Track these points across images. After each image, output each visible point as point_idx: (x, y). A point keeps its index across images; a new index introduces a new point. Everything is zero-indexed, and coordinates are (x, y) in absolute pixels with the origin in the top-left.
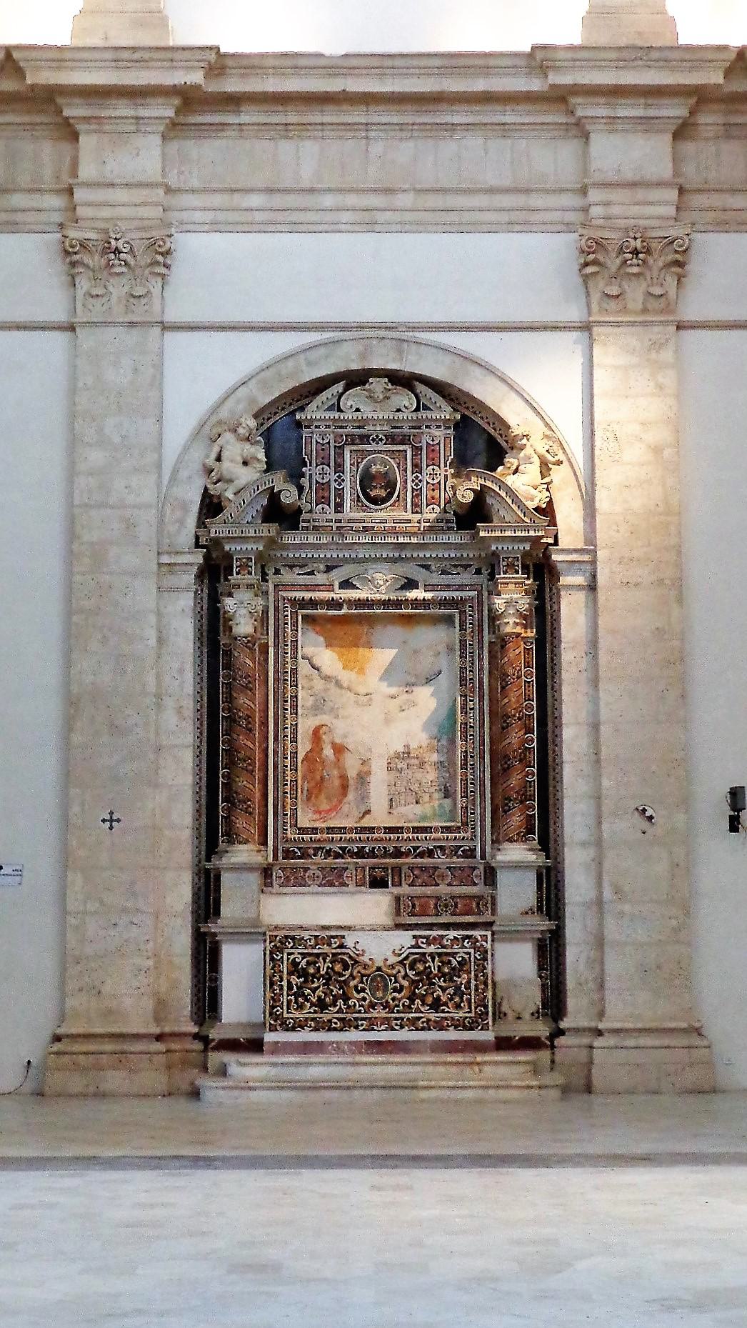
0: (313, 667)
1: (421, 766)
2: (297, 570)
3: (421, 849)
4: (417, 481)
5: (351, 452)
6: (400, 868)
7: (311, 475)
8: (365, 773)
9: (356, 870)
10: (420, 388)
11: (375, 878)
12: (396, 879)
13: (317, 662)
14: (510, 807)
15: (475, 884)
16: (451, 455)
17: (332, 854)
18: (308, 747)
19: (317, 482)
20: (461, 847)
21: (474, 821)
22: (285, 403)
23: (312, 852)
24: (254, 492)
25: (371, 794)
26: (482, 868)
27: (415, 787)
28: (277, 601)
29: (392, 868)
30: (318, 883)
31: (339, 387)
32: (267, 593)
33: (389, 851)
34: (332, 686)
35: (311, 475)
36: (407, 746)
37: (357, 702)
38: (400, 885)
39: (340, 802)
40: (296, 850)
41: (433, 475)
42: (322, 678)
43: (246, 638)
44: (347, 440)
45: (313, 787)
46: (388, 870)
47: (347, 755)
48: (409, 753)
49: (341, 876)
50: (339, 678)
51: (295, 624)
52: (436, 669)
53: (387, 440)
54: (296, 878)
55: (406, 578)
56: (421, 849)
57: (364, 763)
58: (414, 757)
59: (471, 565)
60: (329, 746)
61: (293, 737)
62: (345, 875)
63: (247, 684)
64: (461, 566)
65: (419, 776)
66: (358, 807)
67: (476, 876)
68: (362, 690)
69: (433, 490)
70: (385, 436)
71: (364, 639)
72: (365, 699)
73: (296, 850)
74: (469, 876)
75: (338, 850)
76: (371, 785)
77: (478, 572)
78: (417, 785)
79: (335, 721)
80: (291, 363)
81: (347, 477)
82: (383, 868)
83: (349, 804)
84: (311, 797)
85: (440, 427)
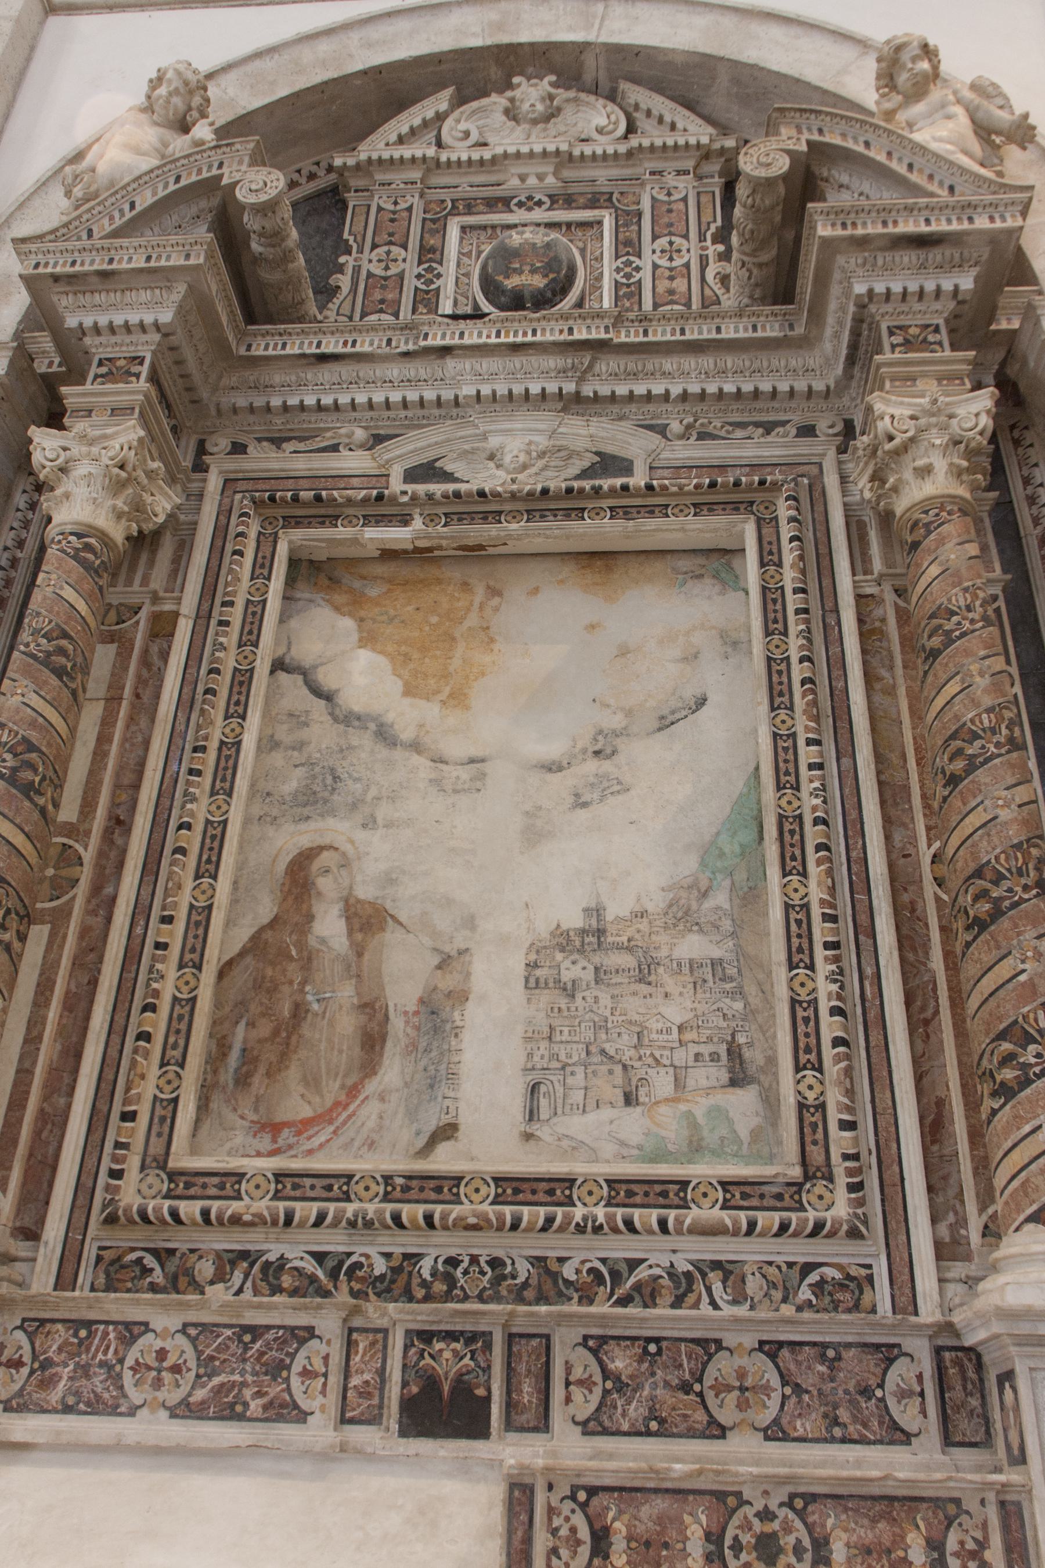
0: (317, 692)
1: (644, 973)
2: (290, 447)
3: (642, 1273)
4: (628, 270)
5: (463, 229)
6: (548, 1337)
7: (357, 269)
8: (449, 995)
9: (350, 1345)
10: (636, 95)
11: (431, 1383)
12: (527, 1392)
13: (327, 678)
14: (1025, 1067)
15: (905, 1438)
16: (715, 221)
17: (286, 1281)
18: (265, 909)
19: (370, 275)
20: (807, 1268)
21: (856, 1157)
22: (318, 164)
23: (206, 1269)
24: (166, 186)
25: (464, 1069)
26: (921, 1348)
27: (622, 1045)
28: (225, 513)
29: (511, 1338)
30: (174, 1397)
31: (441, 102)
32: (201, 496)
33: (514, 1277)
34: (363, 740)
35: (357, 269)
36: (596, 911)
37: (437, 782)
38: (542, 1425)
39: (353, 1091)
40: (150, 1261)
41: (671, 251)
42: (336, 719)
43: (79, 536)
44: (454, 207)
45: (260, 1041)
46: (488, 1346)
47: (392, 936)
48: (600, 932)
49: (278, 1369)
50: (390, 717)
51: (262, 568)
52: (690, 692)
53: (553, 202)
54: (84, 1371)
55: (597, 453)
56: (642, 1273)
57: (445, 963)
58: (619, 947)
59: (783, 424)
60: (336, 910)
61: (209, 861)
62: (297, 1367)
63: (49, 654)
64: (757, 425)
65: (633, 1006)
66: (412, 1114)
67: (903, 1395)
68: (457, 748)
69: (671, 278)
70: (550, 196)
71: (473, 620)
72: (464, 774)
73: (150, 1261)
74: (866, 1392)
75: (310, 1266)
76: (466, 1036)
77: (807, 431)
78: (628, 1039)
79: (360, 835)
80: (324, 47)
81: (449, 269)
82: (471, 1338)
83: (382, 1099)
84: (249, 1075)
85: (686, 172)
